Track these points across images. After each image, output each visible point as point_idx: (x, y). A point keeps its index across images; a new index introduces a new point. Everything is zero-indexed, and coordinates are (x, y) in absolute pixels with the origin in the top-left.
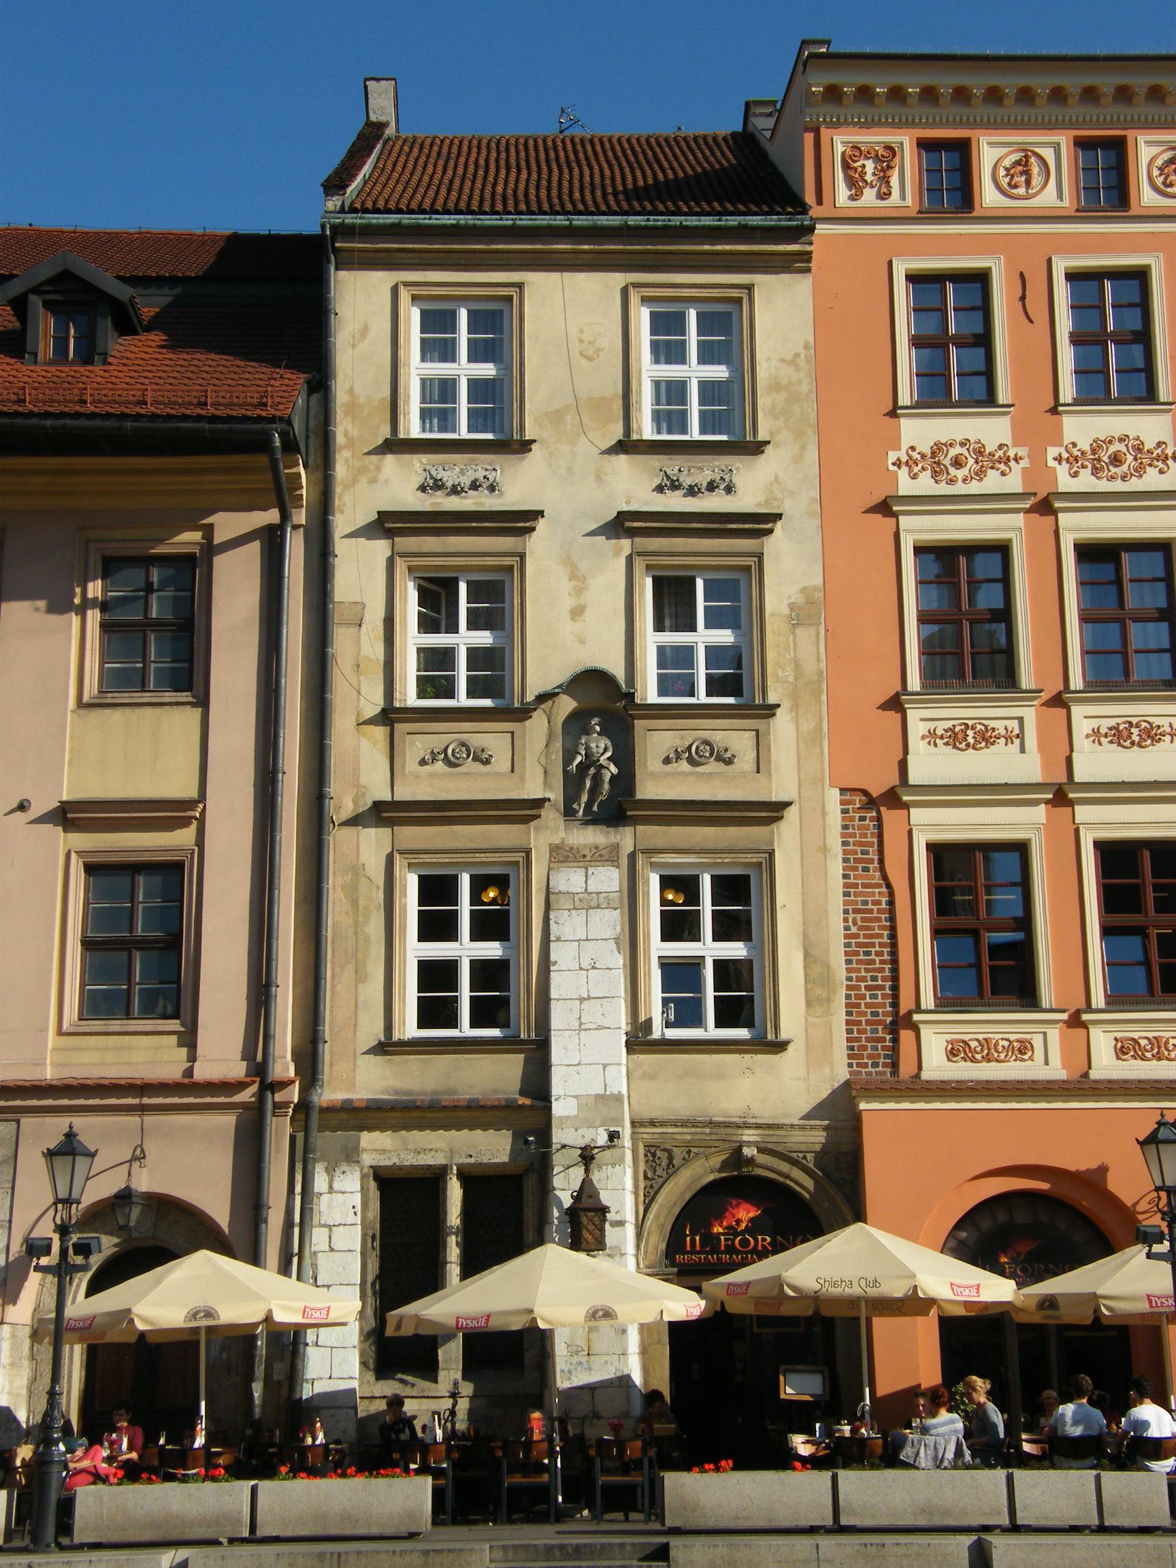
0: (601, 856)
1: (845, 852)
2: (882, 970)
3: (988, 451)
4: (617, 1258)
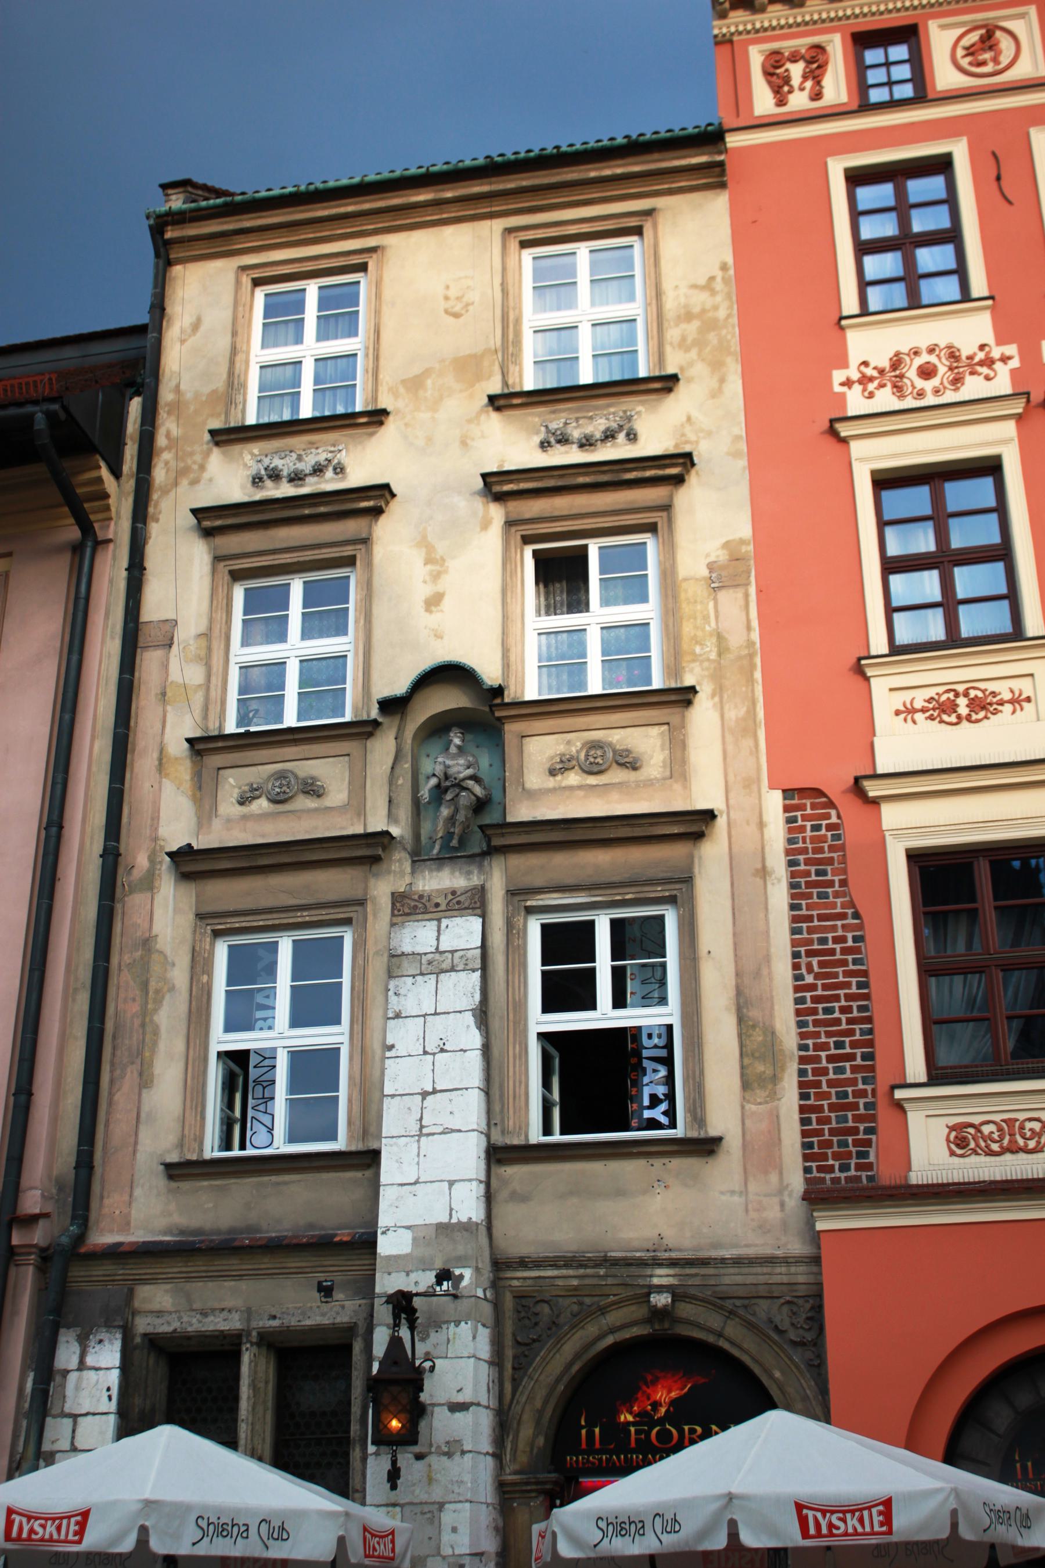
0: (459, 903)
1: (793, 875)
2: (850, 1033)
3: (964, 354)
4: (457, 1457)
